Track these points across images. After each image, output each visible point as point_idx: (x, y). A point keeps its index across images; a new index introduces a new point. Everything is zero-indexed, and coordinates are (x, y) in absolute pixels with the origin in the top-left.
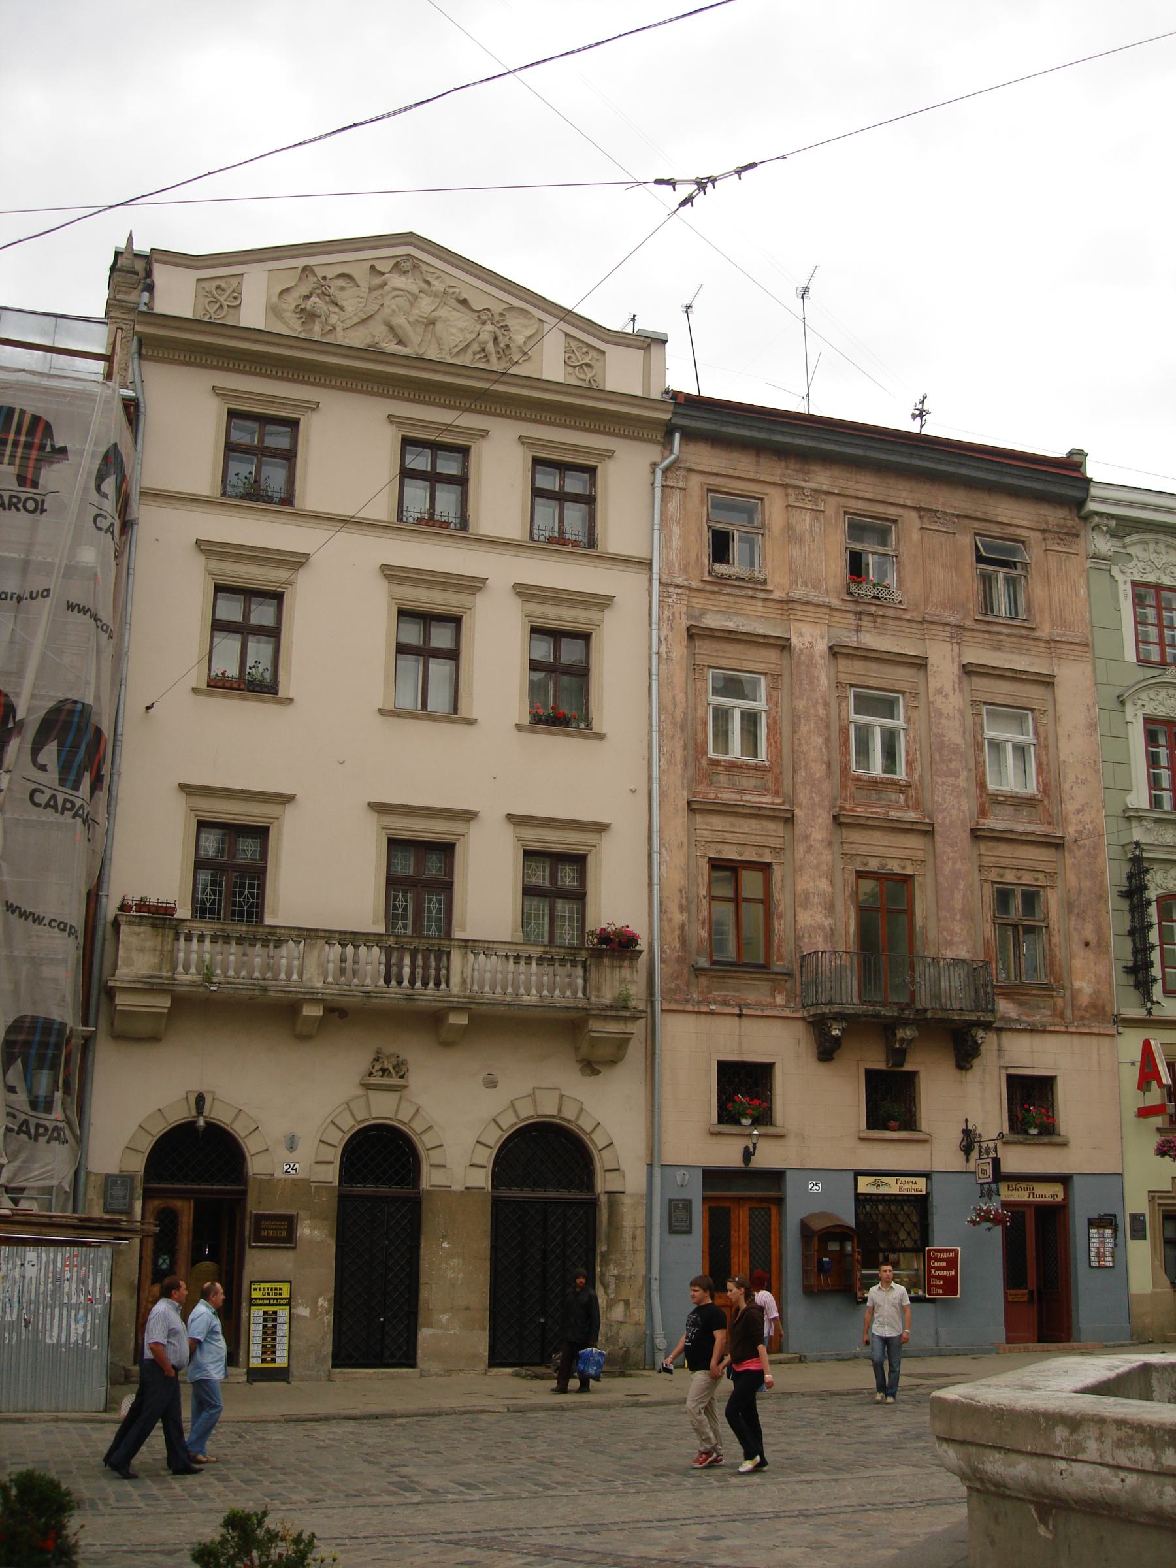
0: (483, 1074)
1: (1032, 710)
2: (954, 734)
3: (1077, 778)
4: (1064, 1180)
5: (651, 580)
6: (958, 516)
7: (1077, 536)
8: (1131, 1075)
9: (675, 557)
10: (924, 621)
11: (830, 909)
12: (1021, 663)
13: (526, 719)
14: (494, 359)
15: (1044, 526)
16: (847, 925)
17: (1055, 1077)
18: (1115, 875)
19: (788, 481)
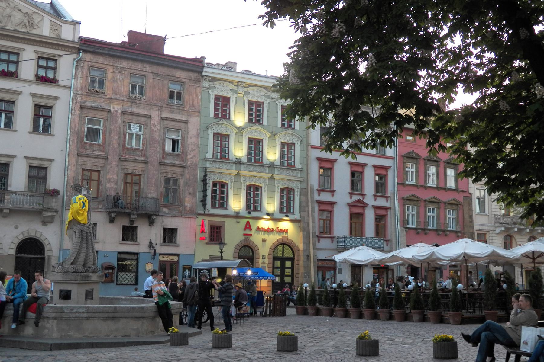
0: (15, 225)
1: (181, 130)
2: (156, 136)
3: (192, 149)
4: (178, 255)
5: (71, 92)
6: (164, 75)
7: (200, 81)
8: (199, 229)
9: (79, 87)
10: (151, 105)
11: (116, 183)
12: (179, 117)
13: (32, 130)
14: (28, 27)
15: (190, 79)
16: (121, 187)
17: (177, 229)
18: (200, 175)
19: (114, 64)
